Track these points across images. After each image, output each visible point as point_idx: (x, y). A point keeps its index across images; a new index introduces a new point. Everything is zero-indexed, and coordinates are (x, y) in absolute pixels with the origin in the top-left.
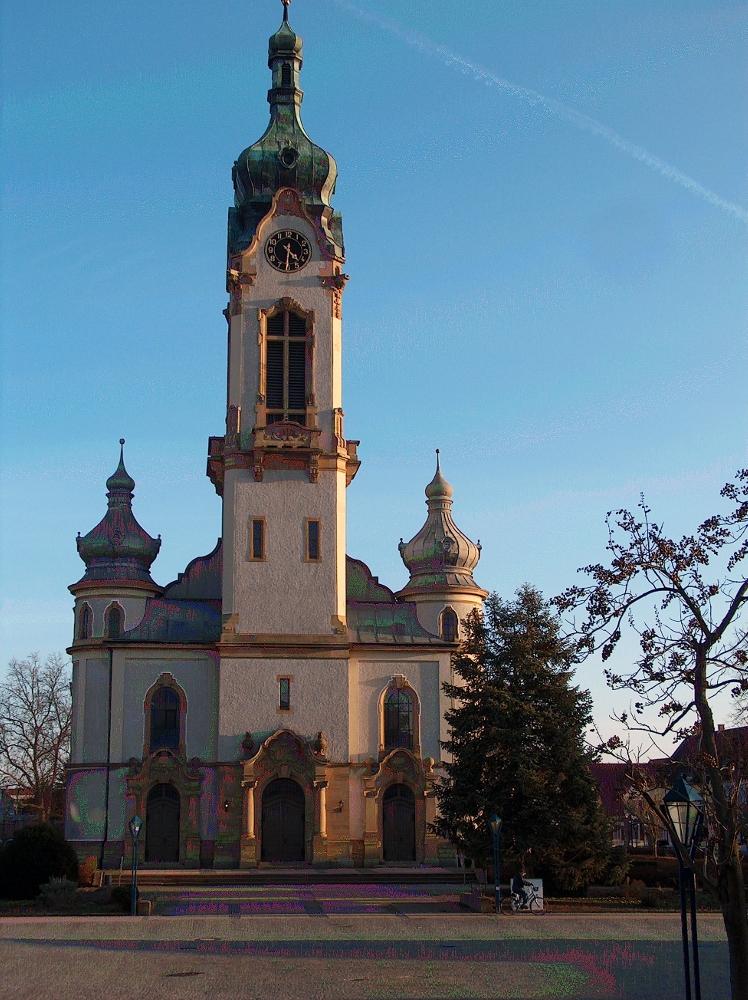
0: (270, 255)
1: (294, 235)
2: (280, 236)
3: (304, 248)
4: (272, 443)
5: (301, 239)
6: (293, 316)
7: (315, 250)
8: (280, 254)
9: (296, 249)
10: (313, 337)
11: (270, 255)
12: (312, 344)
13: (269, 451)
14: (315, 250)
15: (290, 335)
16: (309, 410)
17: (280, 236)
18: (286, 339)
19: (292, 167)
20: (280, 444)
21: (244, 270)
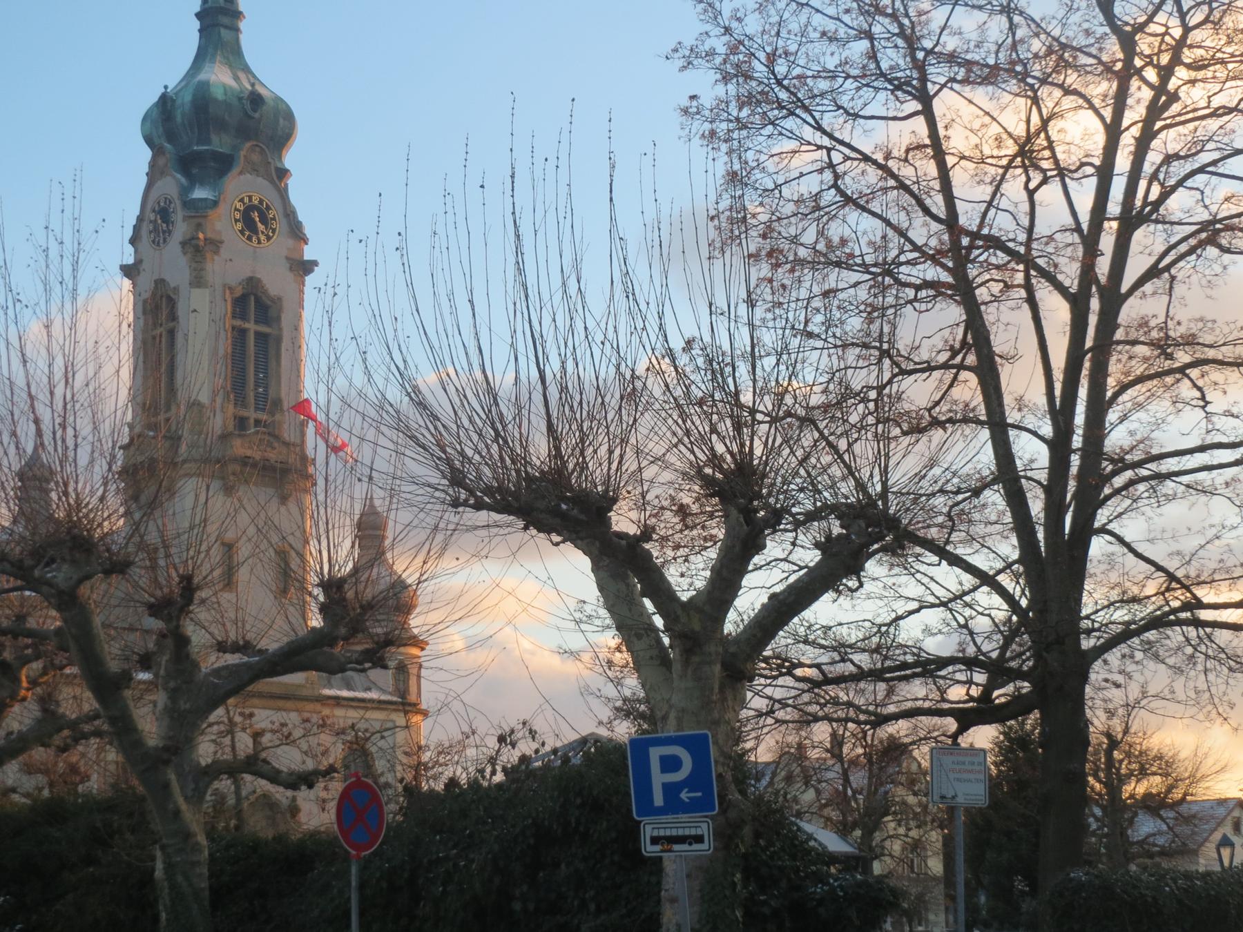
0: (236, 221)
1: (261, 201)
2: (246, 200)
3: (272, 219)
4: (249, 453)
5: (268, 208)
6: (258, 300)
7: (280, 225)
8: (249, 225)
9: (264, 220)
10: (280, 329)
11: (236, 221)
12: (279, 340)
13: (244, 461)
14: (280, 225)
15: (256, 322)
16: (278, 417)
17: (246, 200)
18: (251, 326)
19: (257, 115)
20: (257, 456)
21: (209, 235)
